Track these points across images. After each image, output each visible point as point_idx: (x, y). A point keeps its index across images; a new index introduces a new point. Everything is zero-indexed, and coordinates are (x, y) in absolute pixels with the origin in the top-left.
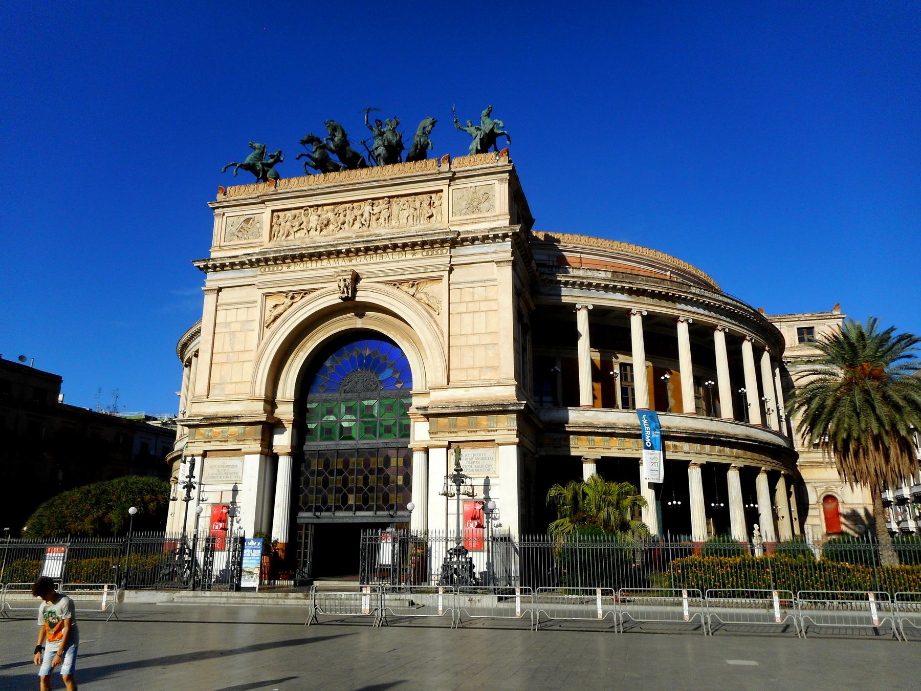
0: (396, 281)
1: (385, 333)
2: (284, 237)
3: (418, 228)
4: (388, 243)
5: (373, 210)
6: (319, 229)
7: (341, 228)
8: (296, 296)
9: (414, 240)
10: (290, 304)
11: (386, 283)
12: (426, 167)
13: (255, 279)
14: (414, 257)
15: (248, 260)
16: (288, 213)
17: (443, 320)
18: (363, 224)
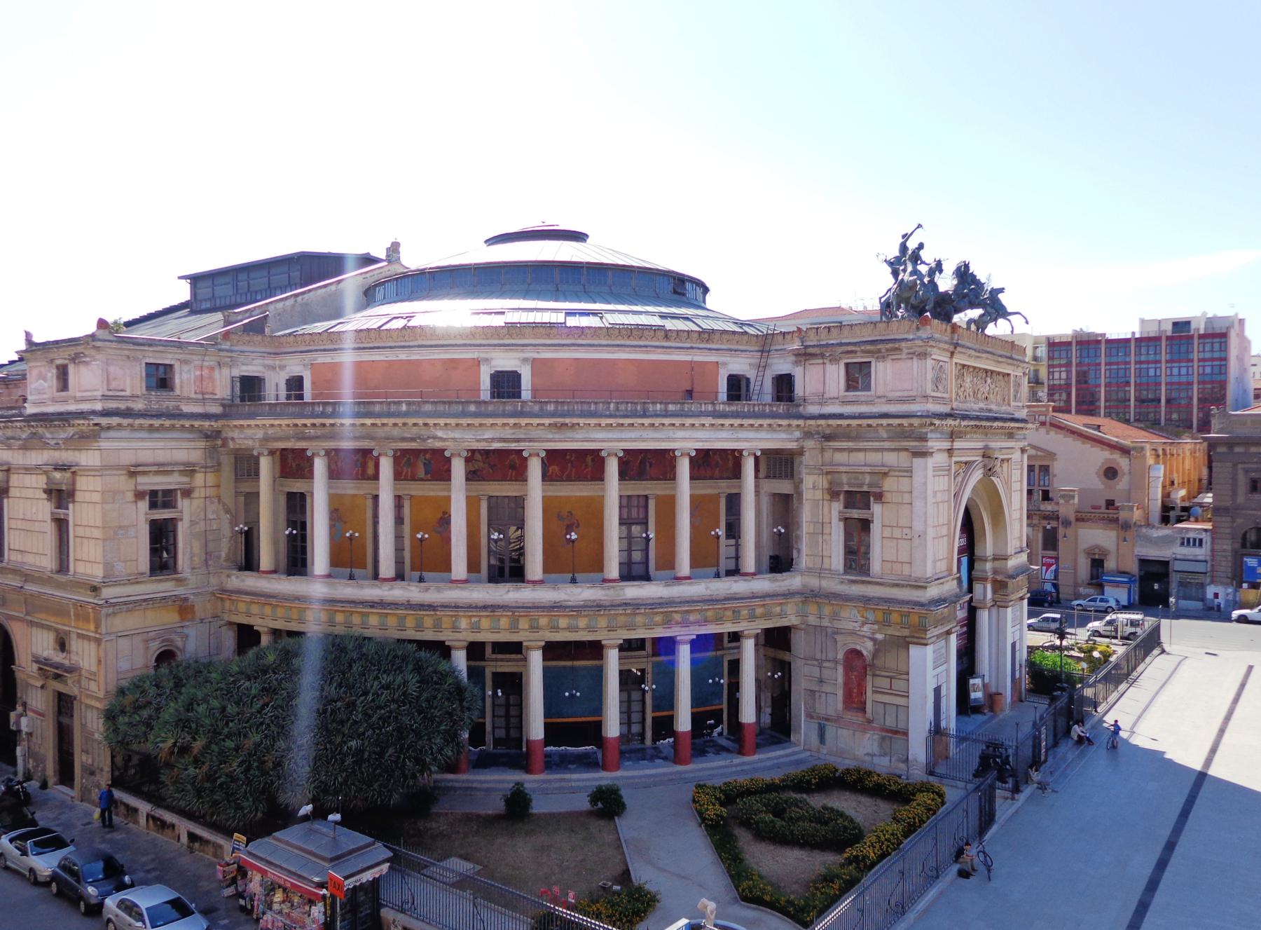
1: (979, 503)
13: (950, 444)
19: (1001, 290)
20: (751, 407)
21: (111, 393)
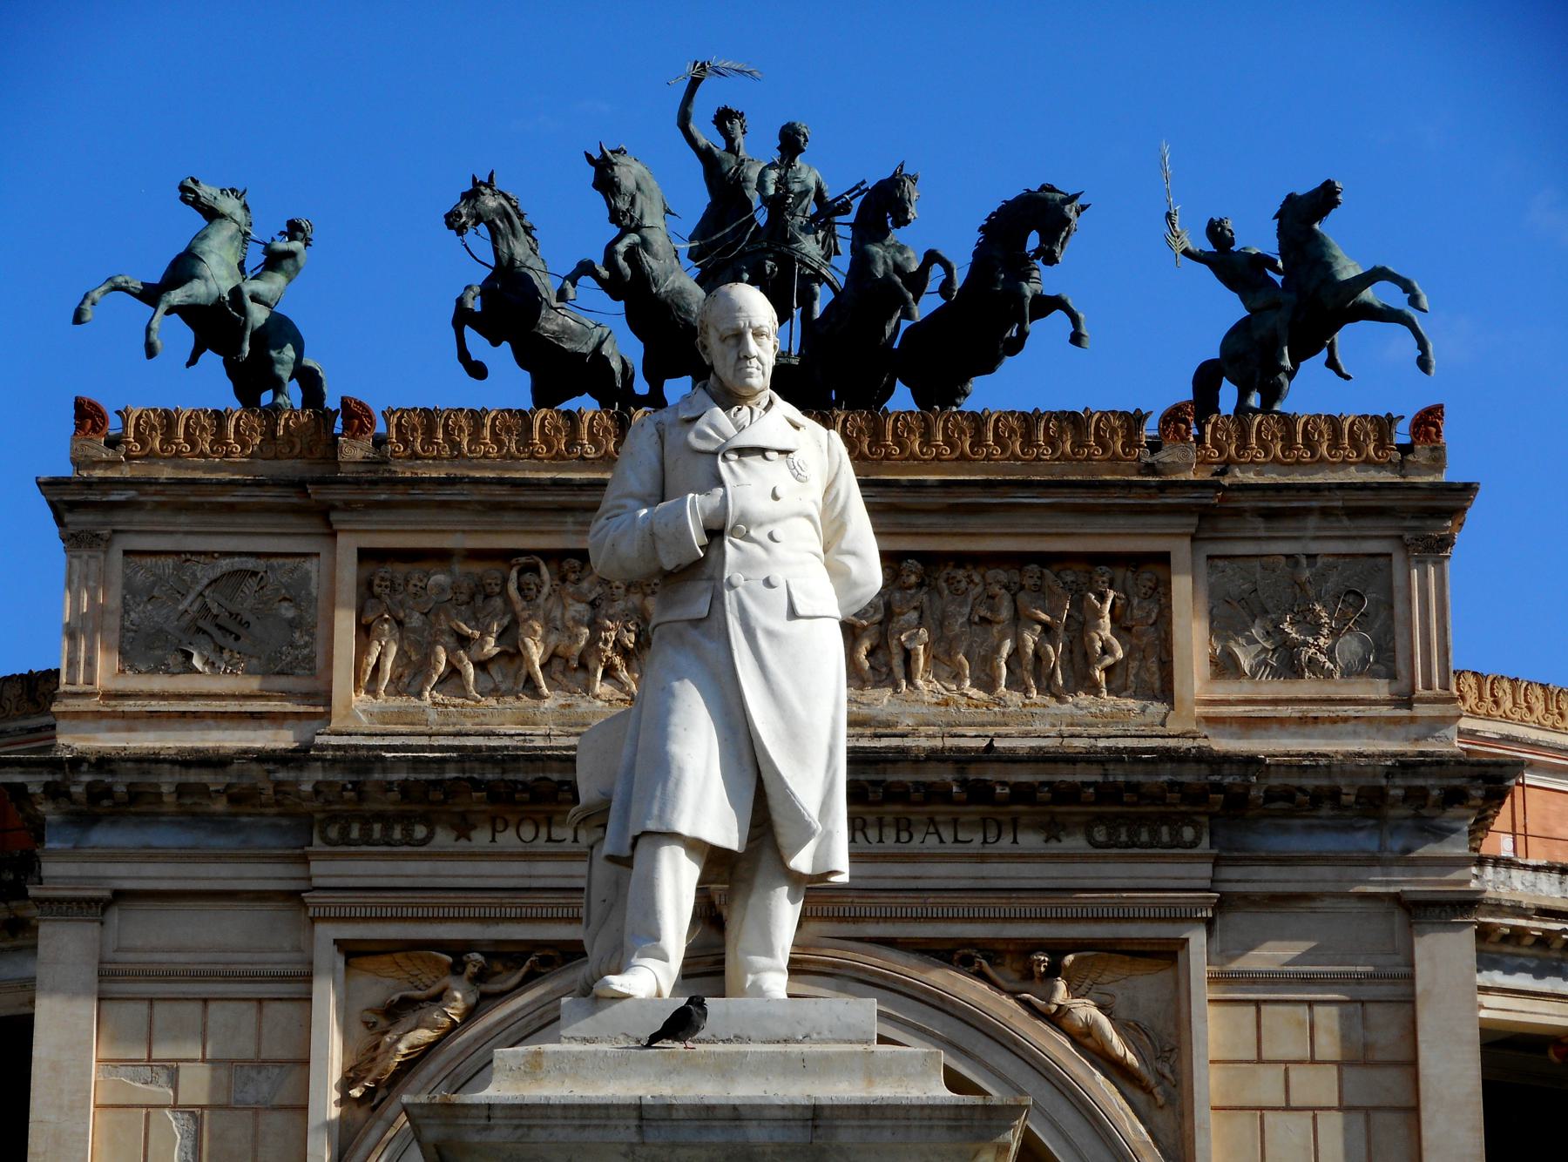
0: (970, 943)
4: (949, 777)
8: (498, 967)
9: (1069, 778)
13: (296, 870)
14: (1054, 847)
15: (278, 784)
16: (440, 578)
19: (1325, 198)
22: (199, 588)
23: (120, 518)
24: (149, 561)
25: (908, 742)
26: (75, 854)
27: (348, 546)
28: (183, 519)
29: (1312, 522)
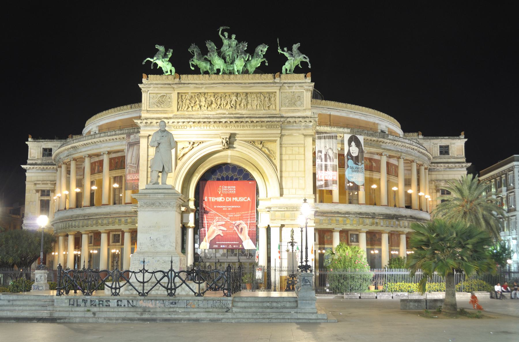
2: (185, 109)
3: (262, 112)
5: (237, 99)
6: (206, 106)
7: (219, 107)
10: (191, 148)
11: (245, 141)
12: (267, 77)
14: (261, 128)
17: (277, 162)
18: (232, 107)
20: (129, 130)
21: (31, 158)
22: (158, 97)
23: (148, 89)
24: (152, 94)
25: (244, 116)
26: (144, 130)
27: (176, 92)
28: (156, 89)
29: (294, 87)
